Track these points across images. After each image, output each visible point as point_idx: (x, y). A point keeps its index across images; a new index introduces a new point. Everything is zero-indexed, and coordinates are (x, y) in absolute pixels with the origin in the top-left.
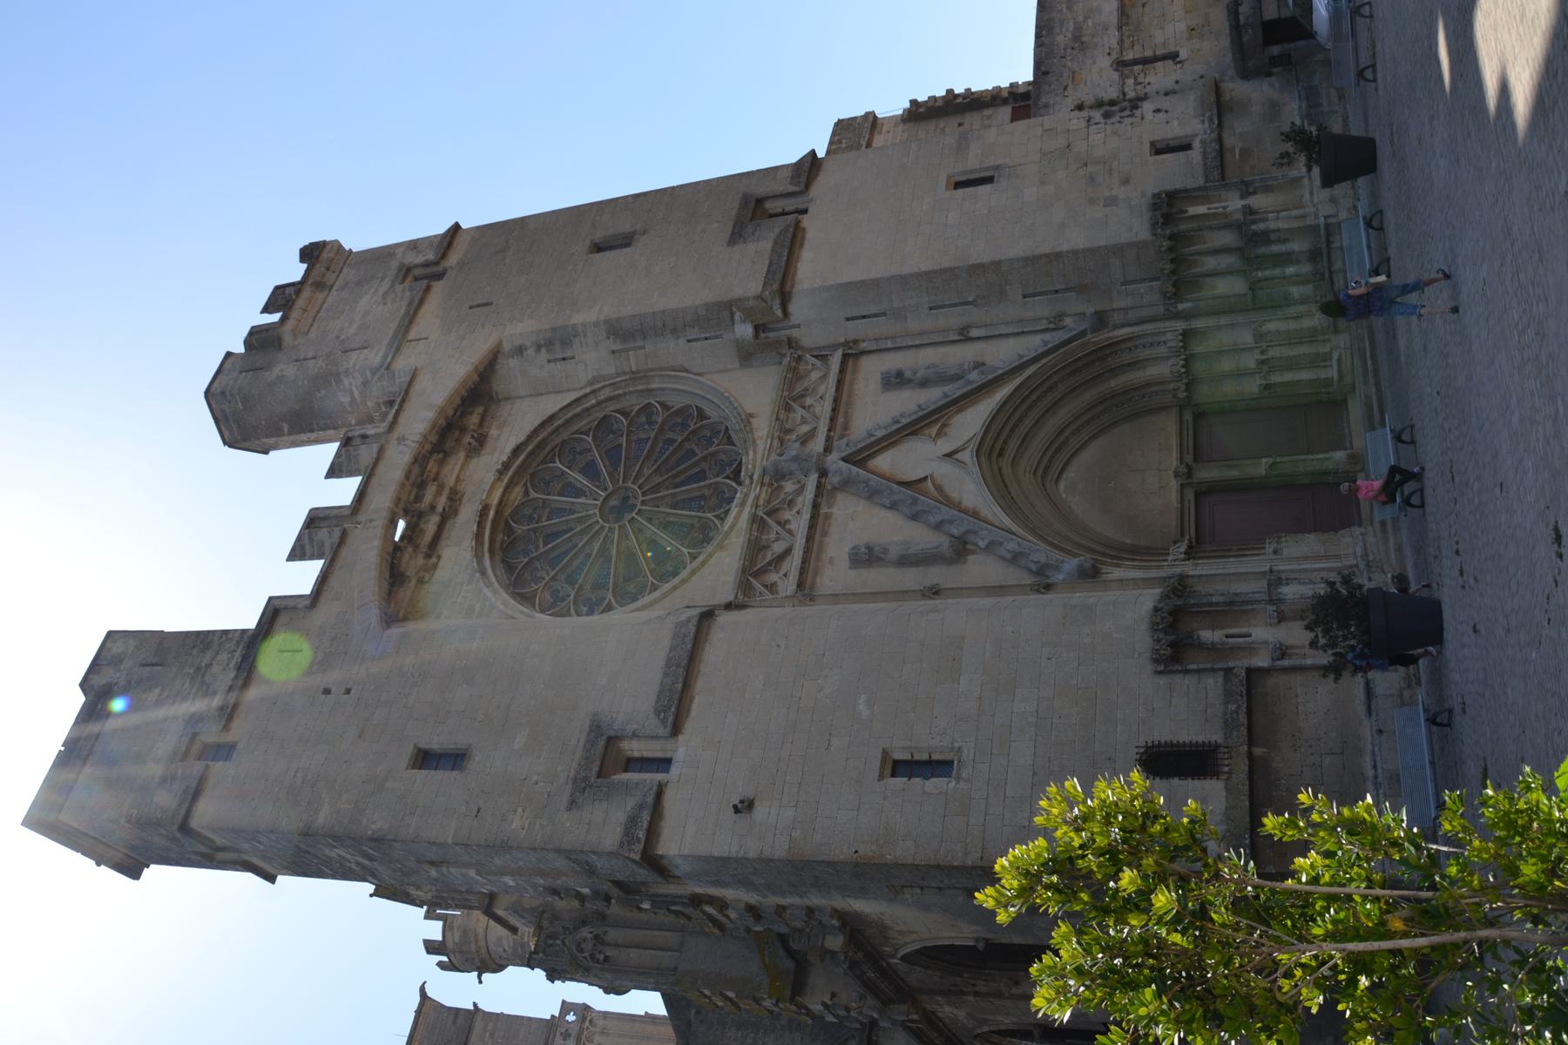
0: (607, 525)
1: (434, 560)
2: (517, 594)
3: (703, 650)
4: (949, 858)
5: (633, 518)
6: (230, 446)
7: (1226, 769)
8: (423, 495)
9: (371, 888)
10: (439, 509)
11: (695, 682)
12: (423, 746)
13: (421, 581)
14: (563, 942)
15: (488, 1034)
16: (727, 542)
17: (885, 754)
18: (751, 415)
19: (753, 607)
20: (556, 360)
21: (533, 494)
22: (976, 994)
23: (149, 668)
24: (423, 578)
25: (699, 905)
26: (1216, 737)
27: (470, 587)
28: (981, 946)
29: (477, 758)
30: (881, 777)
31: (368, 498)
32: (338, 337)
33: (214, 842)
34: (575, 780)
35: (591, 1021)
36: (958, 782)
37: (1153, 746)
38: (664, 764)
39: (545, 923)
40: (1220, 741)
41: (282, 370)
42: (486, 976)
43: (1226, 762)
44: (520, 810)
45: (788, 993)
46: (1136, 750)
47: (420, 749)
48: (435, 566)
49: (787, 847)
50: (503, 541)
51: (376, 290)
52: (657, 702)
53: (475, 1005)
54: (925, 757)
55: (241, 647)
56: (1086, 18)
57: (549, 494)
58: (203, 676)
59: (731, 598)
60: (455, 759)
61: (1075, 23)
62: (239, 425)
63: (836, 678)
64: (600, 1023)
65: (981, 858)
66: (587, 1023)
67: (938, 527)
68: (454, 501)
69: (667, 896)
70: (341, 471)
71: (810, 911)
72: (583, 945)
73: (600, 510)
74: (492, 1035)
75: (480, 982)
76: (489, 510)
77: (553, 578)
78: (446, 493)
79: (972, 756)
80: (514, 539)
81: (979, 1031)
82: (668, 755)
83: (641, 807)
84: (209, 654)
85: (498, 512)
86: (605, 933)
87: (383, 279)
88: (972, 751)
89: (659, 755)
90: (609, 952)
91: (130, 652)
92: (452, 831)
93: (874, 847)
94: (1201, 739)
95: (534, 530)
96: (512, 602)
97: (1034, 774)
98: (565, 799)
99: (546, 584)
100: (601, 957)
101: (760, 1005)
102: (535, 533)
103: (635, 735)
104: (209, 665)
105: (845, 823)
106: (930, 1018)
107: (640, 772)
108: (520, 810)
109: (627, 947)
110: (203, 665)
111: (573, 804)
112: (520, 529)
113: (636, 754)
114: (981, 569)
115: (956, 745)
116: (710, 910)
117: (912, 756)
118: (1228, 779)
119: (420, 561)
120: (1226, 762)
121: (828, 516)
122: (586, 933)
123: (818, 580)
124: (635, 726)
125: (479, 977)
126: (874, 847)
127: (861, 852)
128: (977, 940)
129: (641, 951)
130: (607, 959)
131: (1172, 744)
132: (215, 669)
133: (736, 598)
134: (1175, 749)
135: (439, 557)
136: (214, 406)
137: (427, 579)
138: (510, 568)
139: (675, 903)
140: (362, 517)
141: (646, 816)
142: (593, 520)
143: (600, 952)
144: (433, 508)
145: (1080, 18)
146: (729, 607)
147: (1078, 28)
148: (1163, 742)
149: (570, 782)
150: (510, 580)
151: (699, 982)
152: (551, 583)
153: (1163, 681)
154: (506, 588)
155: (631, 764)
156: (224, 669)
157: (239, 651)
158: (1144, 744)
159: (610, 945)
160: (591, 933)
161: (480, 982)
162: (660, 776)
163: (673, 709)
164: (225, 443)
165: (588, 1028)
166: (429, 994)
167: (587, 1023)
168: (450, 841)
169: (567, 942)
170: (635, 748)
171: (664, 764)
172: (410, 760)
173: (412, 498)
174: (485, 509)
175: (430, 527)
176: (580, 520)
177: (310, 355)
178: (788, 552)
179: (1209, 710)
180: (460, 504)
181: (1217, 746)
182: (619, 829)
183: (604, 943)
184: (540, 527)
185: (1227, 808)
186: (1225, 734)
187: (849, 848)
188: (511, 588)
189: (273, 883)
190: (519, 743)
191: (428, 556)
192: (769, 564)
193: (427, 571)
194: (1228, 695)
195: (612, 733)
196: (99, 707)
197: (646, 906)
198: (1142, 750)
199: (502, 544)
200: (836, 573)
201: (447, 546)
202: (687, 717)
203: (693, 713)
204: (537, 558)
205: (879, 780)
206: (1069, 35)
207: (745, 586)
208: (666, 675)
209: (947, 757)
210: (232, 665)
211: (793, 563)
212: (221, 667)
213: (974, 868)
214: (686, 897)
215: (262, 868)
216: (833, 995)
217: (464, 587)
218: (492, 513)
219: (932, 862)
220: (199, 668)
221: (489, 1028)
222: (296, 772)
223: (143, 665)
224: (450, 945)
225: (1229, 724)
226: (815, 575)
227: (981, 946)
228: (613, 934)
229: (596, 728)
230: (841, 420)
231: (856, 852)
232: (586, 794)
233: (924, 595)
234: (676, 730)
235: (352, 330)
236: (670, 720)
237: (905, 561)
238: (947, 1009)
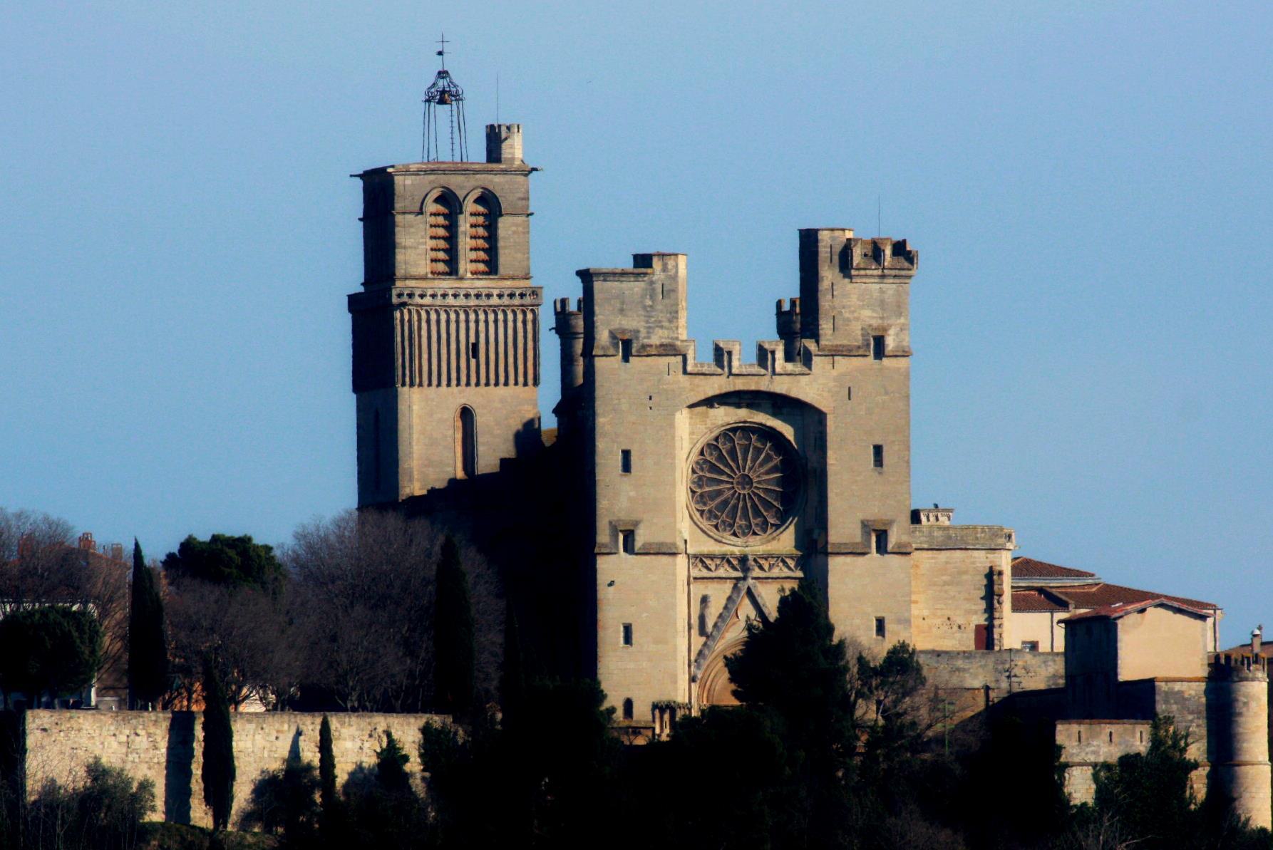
18: (779, 540)
20: (816, 440)
31: (741, 377)
32: (844, 308)
41: (827, 277)
51: (874, 318)
53: (532, 214)
55: (670, 341)
56: (971, 674)
58: (657, 326)
60: (627, 467)
61: (969, 669)
67: (715, 625)
75: (550, 330)
84: (666, 324)
87: (882, 318)
91: (669, 273)
104: (662, 327)
114: (698, 641)
121: (726, 582)
125: (553, 328)
132: (660, 331)
141: (608, 551)
145: (971, 671)
147: (964, 670)
161: (550, 330)
177: (835, 293)
178: (709, 570)
190: (632, 494)
194: (648, 722)
200: (699, 590)
206: (962, 666)
207: (696, 556)
208: (657, 544)
210: (663, 340)
211: (705, 573)
220: (660, 322)
225: (637, 722)
230: (770, 580)
235: (847, 315)
237: (702, 619)
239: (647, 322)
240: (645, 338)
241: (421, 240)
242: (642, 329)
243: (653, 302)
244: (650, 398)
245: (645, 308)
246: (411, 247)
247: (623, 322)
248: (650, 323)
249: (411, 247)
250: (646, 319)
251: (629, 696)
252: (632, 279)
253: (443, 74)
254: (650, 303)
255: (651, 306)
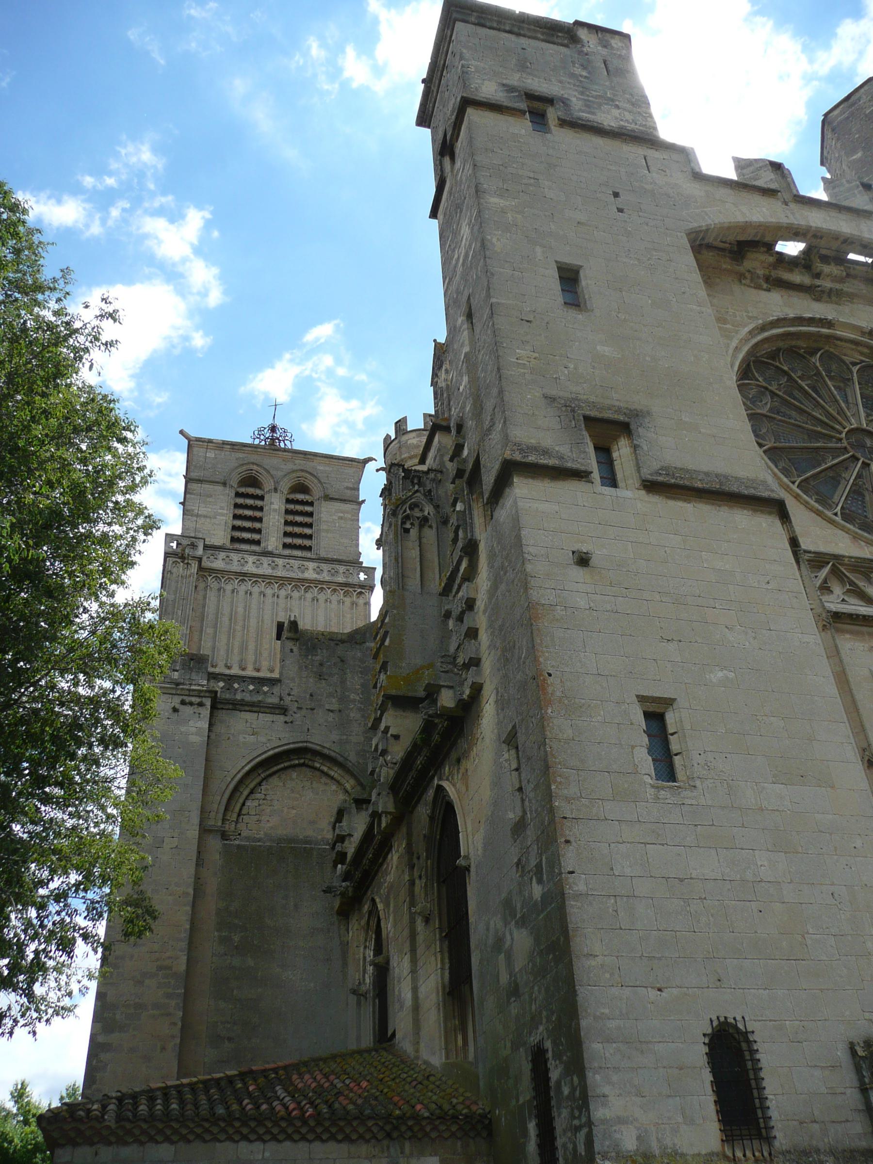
0: (843, 435)
1: (765, 286)
2: (748, 365)
3: (745, 508)
4: (559, 779)
5: (858, 460)
6: (823, 122)
7: (739, 1154)
8: (829, 264)
9: (442, 339)
10: (817, 282)
11: (706, 503)
12: (582, 274)
13: (741, 277)
14: (417, 491)
15: (342, 515)
16: (863, 543)
17: (669, 702)
19: (799, 569)
21: (855, 369)
22: (412, 883)
23: (603, 65)
24: (745, 278)
25: (466, 554)
26: (782, 1139)
27: (746, 318)
28: (461, 862)
29: (580, 316)
30: (642, 699)
33: (457, 141)
34: (576, 399)
35: (361, 593)
36: (653, 786)
37: (748, 1042)
38: (611, 481)
39: (432, 475)
40: (777, 1143)
42: (383, 474)
43: (749, 1154)
44: (537, 355)
45: (393, 692)
46: (739, 1018)
47: (578, 272)
48: (758, 287)
49: (543, 602)
50: (799, 348)
52: (675, 468)
53: (363, 501)
54: (674, 747)
55: (641, 128)
57: (859, 384)
58: (606, 104)
59: (803, 546)
62: (848, 118)
63: (747, 643)
64: (361, 601)
65: (565, 818)
66: (359, 590)
68: (829, 296)
69: (471, 518)
70: (834, 188)
71: (475, 662)
72: (417, 510)
73: (857, 429)
74: (341, 518)
75: (378, 470)
76: (829, 328)
77: (773, 394)
78: (838, 286)
79: (687, 801)
80: (804, 357)
81: (378, 900)
82: (621, 484)
83: (561, 458)
85: (828, 337)
86: (431, 527)
88: (694, 802)
89: (619, 476)
90: (414, 532)
92: (503, 301)
93: (558, 694)
94: (774, 1113)
95: (818, 374)
96: (741, 356)
97: (681, 880)
98: (554, 392)
99: (766, 388)
100: (408, 526)
101: (380, 672)
102: (815, 375)
103: (635, 447)
104: (617, 107)
105: (580, 662)
106: (384, 848)
107: (598, 462)
108: (537, 355)
109: (420, 546)
110: (617, 103)
111: (551, 400)
112: (816, 360)
113: (615, 455)
115: (698, 783)
116: (464, 565)
117: (672, 734)
118: (726, 1157)
119: (760, 272)
120: (749, 1154)
122: (428, 509)
123: (848, 636)
124: (645, 448)
125: (382, 469)
126: (558, 694)
127: (550, 680)
128: (467, 857)
129: (418, 559)
130: (407, 531)
131: (757, 1070)
132: (616, 112)
133: (806, 551)
134: (752, 1076)
135: (769, 290)
136: (862, 90)
137: (743, 282)
138: (774, 355)
139: (465, 532)
140: (793, 206)
141: (551, 462)
142: (845, 423)
143: (412, 524)
144: (818, 276)
146: (794, 542)
148: (758, 1056)
149: (573, 396)
150: (762, 356)
151: (395, 611)
152: (767, 393)
153: (842, 1054)
154: (750, 353)
155: (604, 451)
156: (616, 118)
157: (637, 127)
158: (749, 1029)
159: (420, 532)
160: (429, 514)
161: (378, 470)
162: (596, 476)
163: (673, 481)
164: (826, 115)
165: (355, 591)
166: (367, 465)
167: (359, 590)
168: (493, 300)
169: (418, 494)
170: (622, 451)
171: (611, 481)
172: (566, 264)
173: (824, 252)
174: (829, 324)
175: (797, 277)
176: (841, 412)
179: (816, 1126)
180: (827, 302)
181: (769, 1140)
182: (533, 441)
183: (421, 526)
184: (823, 378)
185: (682, 1155)
186: (789, 1152)
187: (553, 666)
188: (753, 358)
189: (430, 217)
190: (605, 350)
191: (767, 279)
192: (852, 583)
193: (752, 280)
195: (633, 427)
196: (560, 34)
197: (459, 507)
198: (741, 1026)
199: (795, 347)
201: (782, 296)
202: (667, 497)
203: (671, 503)
204: (790, 378)
205: (637, 696)
207: (818, 561)
209: (680, 774)
210: (622, 123)
212: (618, 116)
213: (552, 810)
214: (472, 536)
215: (441, 198)
216: (396, 737)
217: (745, 314)
218: (825, 331)
219: (550, 759)
220: (613, 100)
221: (346, 515)
222: (534, 179)
223: (605, 62)
224: (404, 438)
226: (851, 632)
227: (461, 862)
228: (430, 534)
229: (637, 414)
231: (550, 675)
232: (564, 409)
233: (864, 750)
234: (651, 486)
236: (660, 479)
238: (395, 858)
239: (582, 93)
240: (580, 110)
241: (220, 511)
242: (574, 99)
243: (589, 73)
244: (616, 195)
245: (572, 75)
246: (205, 517)
247: (529, 81)
248: (588, 96)
249: (205, 517)
250: (581, 89)
251: (733, 1014)
252: (539, 36)
253: (273, 429)
254: (584, 73)
255: (586, 77)
